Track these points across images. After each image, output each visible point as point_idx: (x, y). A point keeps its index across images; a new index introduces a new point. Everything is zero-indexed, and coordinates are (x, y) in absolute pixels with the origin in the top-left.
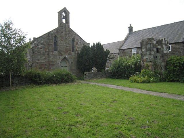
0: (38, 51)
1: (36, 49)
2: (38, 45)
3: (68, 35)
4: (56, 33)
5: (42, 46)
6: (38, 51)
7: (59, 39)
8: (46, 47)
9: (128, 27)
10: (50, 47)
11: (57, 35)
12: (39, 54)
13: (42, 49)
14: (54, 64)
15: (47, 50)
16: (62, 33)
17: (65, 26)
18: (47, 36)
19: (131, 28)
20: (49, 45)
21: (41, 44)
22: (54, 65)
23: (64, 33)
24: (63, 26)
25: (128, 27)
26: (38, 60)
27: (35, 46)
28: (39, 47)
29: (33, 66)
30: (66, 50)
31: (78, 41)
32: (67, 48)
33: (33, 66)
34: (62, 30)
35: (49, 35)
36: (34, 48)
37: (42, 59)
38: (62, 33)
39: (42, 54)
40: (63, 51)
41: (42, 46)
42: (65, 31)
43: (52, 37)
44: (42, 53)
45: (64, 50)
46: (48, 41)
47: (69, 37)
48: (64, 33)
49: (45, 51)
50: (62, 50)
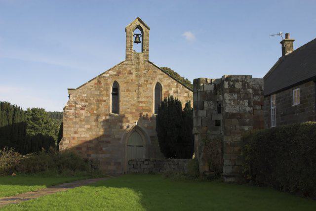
0: (76, 115)
1: (72, 111)
2: (76, 103)
3: (144, 77)
4: (116, 75)
5: (83, 104)
6: (76, 115)
7: (122, 87)
8: (93, 106)
9: (280, 43)
10: (100, 106)
11: (118, 81)
12: (77, 120)
13: (84, 109)
14: (109, 139)
15: (95, 112)
16: (132, 73)
17: (138, 58)
18: (95, 84)
19: (285, 43)
20: (99, 101)
21: (83, 100)
22: (108, 142)
23: (134, 72)
24: (133, 58)
25: (280, 43)
26: (75, 133)
27: (70, 106)
28: (78, 106)
29: (65, 144)
30: (137, 110)
31: (171, 89)
32: (141, 105)
33: (65, 144)
34: (129, 69)
35: (99, 82)
36: (68, 109)
37: (83, 129)
38: (132, 73)
39: (84, 120)
40: (131, 113)
41: (83, 104)
42: (138, 70)
43: (107, 84)
44: (83, 118)
45: (134, 111)
46: (97, 93)
47: (147, 81)
48: (134, 72)
49: (89, 115)
50: (129, 110)
